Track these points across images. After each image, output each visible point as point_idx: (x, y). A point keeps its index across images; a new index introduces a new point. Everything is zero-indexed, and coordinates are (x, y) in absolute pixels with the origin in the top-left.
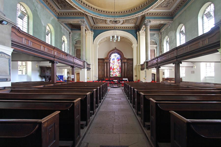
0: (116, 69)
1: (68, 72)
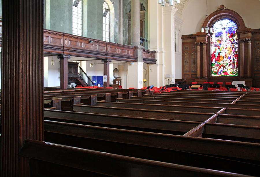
0: (225, 59)
1: (116, 68)
